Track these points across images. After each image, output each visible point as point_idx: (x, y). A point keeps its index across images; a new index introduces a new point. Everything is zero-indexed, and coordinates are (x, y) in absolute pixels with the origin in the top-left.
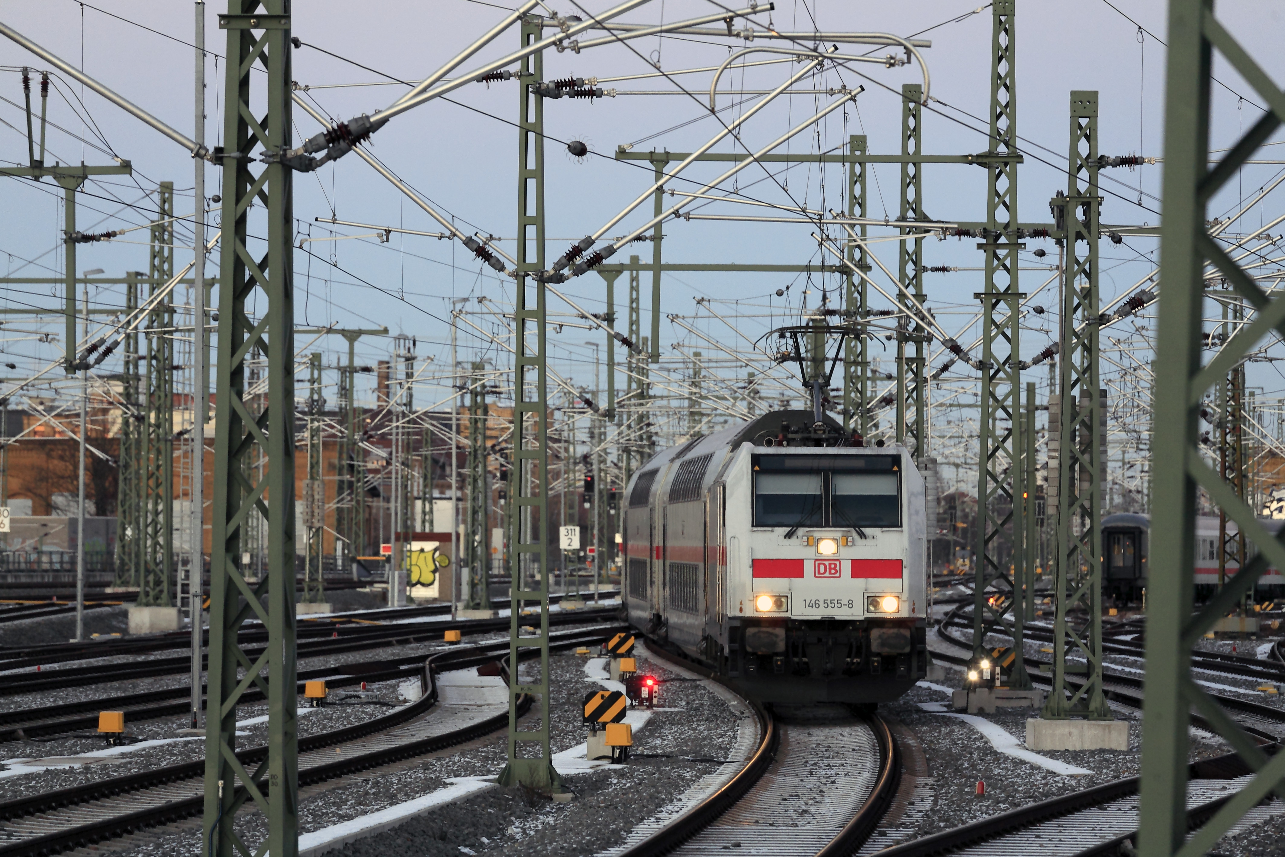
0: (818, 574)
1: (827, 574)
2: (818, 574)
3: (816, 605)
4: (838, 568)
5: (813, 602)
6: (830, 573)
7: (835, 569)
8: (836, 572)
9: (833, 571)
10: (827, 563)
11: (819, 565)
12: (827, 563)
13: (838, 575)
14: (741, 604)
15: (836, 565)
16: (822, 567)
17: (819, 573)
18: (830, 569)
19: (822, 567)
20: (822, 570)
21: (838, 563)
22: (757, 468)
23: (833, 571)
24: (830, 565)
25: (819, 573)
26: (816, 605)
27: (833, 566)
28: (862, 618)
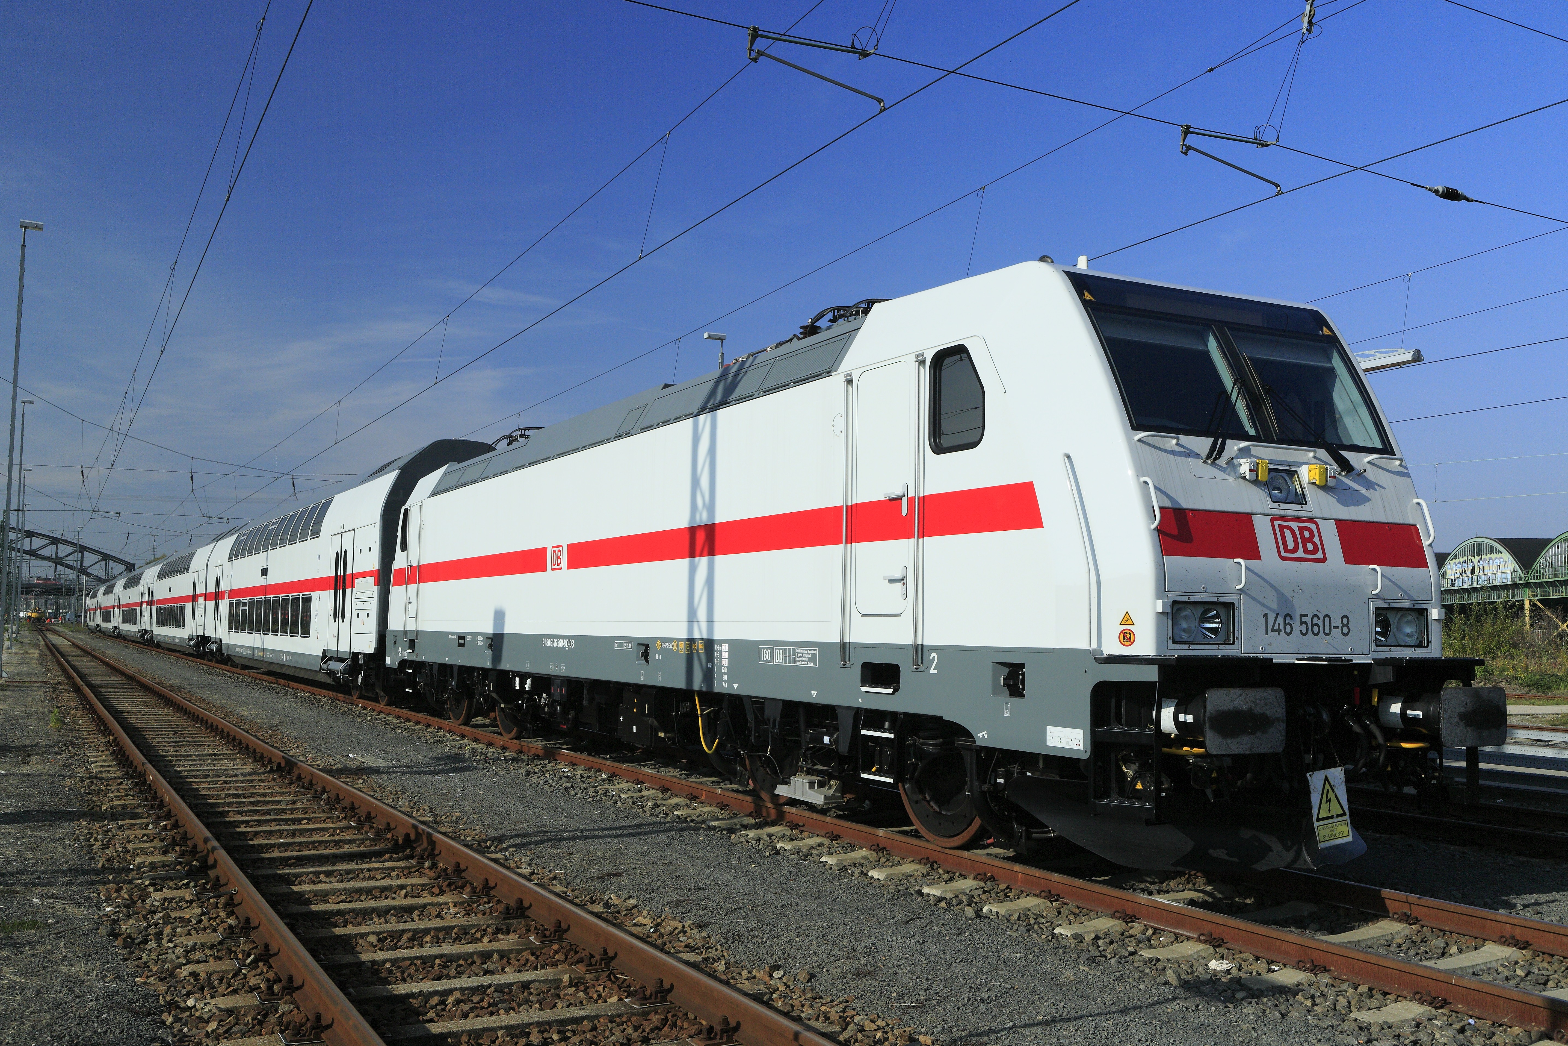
0: (1286, 554)
1: (1300, 553)
4: (1316, 539)
6: (1306, 551)
7: (1311, 539)
8: (1315, 551)
9: (1310, 547)
11: (1282, 528)
12: (1295, 525)
13: (1319, 555)
14: (1127, 619)
17: (1287, 550)
18: (1305, 541)
21: (1312, 526)
22: (1087, 296)
24: (1301, 529)
25: (1287, 550)
27: (1307, 534)
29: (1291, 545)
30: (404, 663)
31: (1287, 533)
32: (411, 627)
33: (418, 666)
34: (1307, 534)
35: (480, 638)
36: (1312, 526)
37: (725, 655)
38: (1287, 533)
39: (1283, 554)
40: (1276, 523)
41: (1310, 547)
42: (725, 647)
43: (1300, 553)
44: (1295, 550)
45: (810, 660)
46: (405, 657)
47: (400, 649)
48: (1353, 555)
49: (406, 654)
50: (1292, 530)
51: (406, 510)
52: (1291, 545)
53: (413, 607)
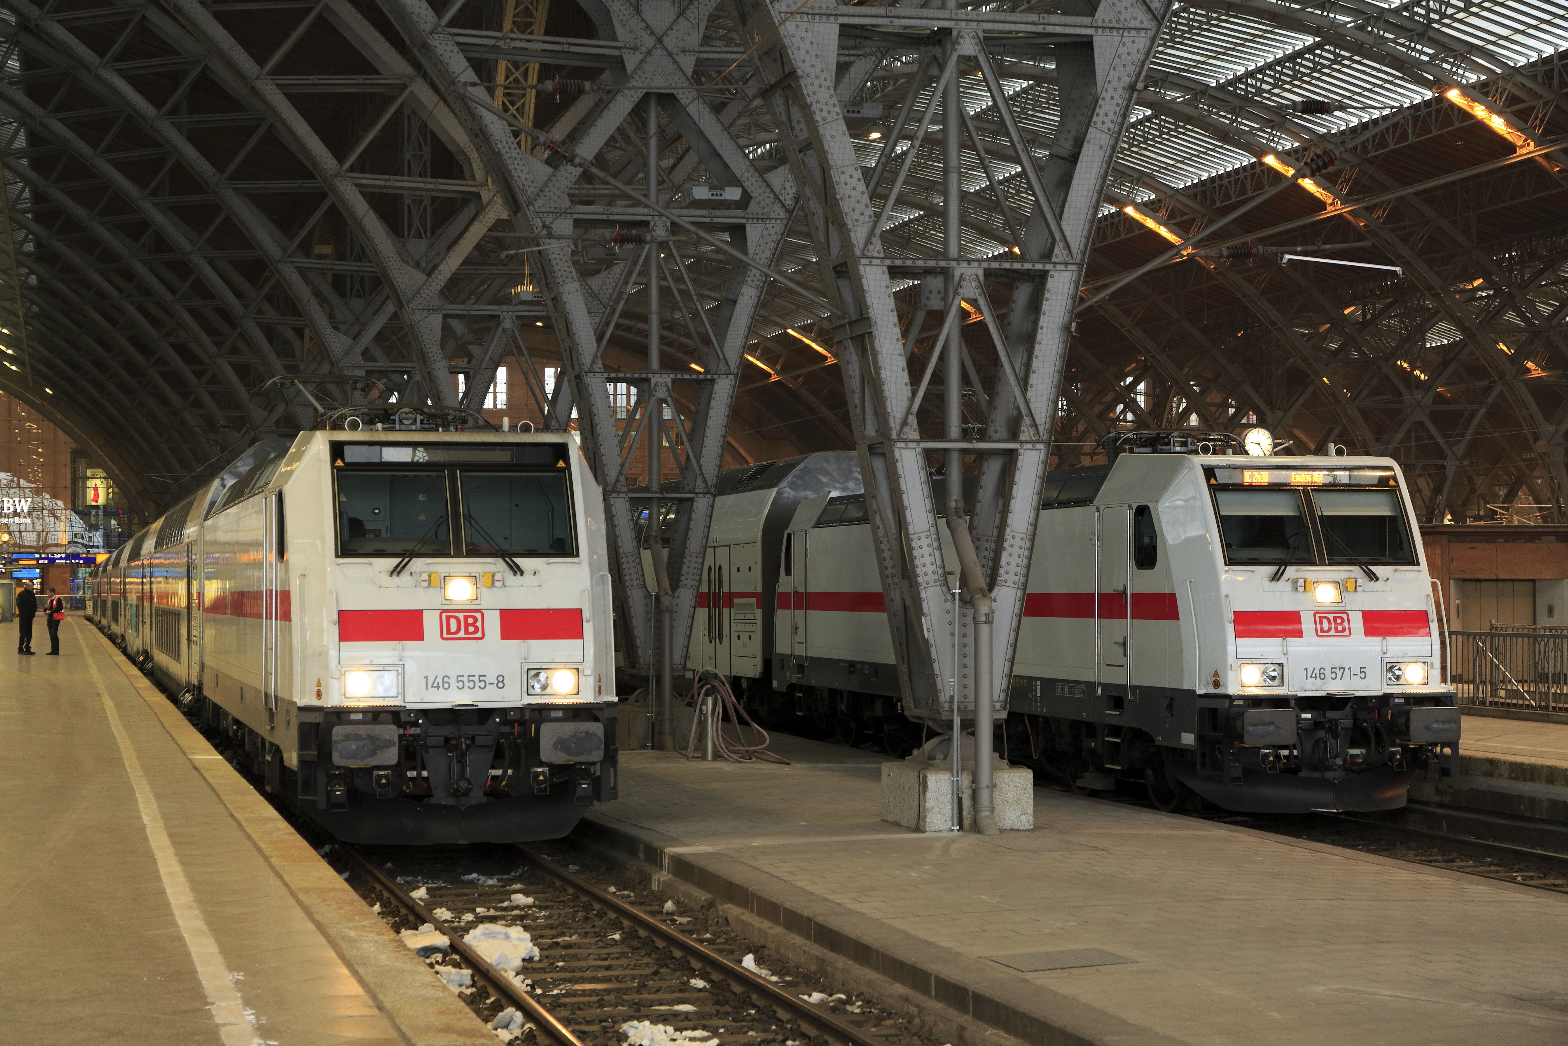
1: (1333, 632)
2: (1321, 633)
3: (1322, 676)
5: (1317, 671)
6: (1336, 630)
8: (1344, 630)
10: (1331, 616)
11: (1321, 618)
12: (1331, 616)
13: (1347, 633)
17: (1322, 630)
20: (1326, 626)
23: (1340, 628)
24: (1335, 618)
26: (1321, 675)
27: (1339, 621)
28: (1380, 693)
30: (792, 687)
31: (1325, 621)
32: (799, 651)
33: (810, 691)
34: (1339, 621)
35: (866, 667)
36: (1345, 616)
37: (1038, 689)
38: (1325, 621)
42: (1038, 683)
43: (1333, 632)
44: (1329, 630)
45: (1082, 693)
46: (794, 681)
47: (788, 674)
48: (1369, 632)
49: (795, 678)
51: (789, 536)
53: (800, 632)
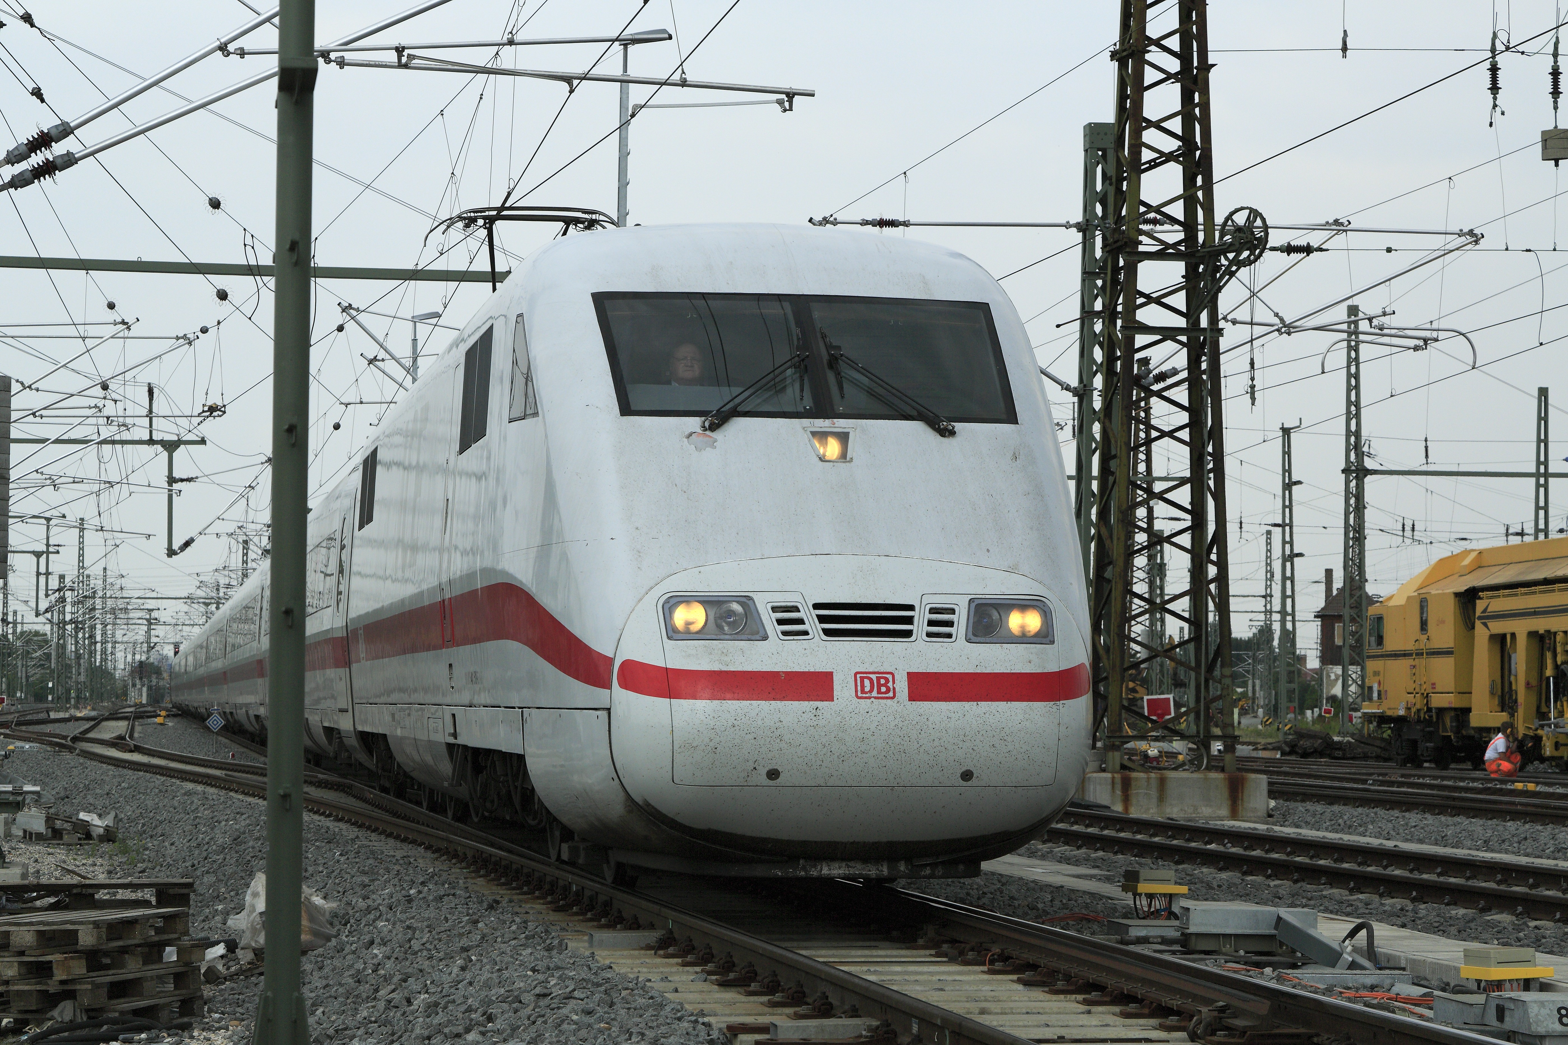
0: (861, 693)
1: (875, 694)
4: (890, 684)
6: (879, 692)
7: (885, 685)
8: (888, 691)
10: (874, 677)
11: (862, 679)
13: (891, 694)
15: (887, 680)
16: (867, 683)
17: (863, 691)
18: (880, 686)
19: (867, 683)
23: (883, 689)
24: (878, 679)
25: (863, 691)
27: (883, 681)
29: (867, 689)
34: (883, 681)
36: (890, 677)
39: (860, 694)
40: (858, 676)
41: (883, 689)
43: (875, 694)
50: (871, 680)
52: (867, 689)
